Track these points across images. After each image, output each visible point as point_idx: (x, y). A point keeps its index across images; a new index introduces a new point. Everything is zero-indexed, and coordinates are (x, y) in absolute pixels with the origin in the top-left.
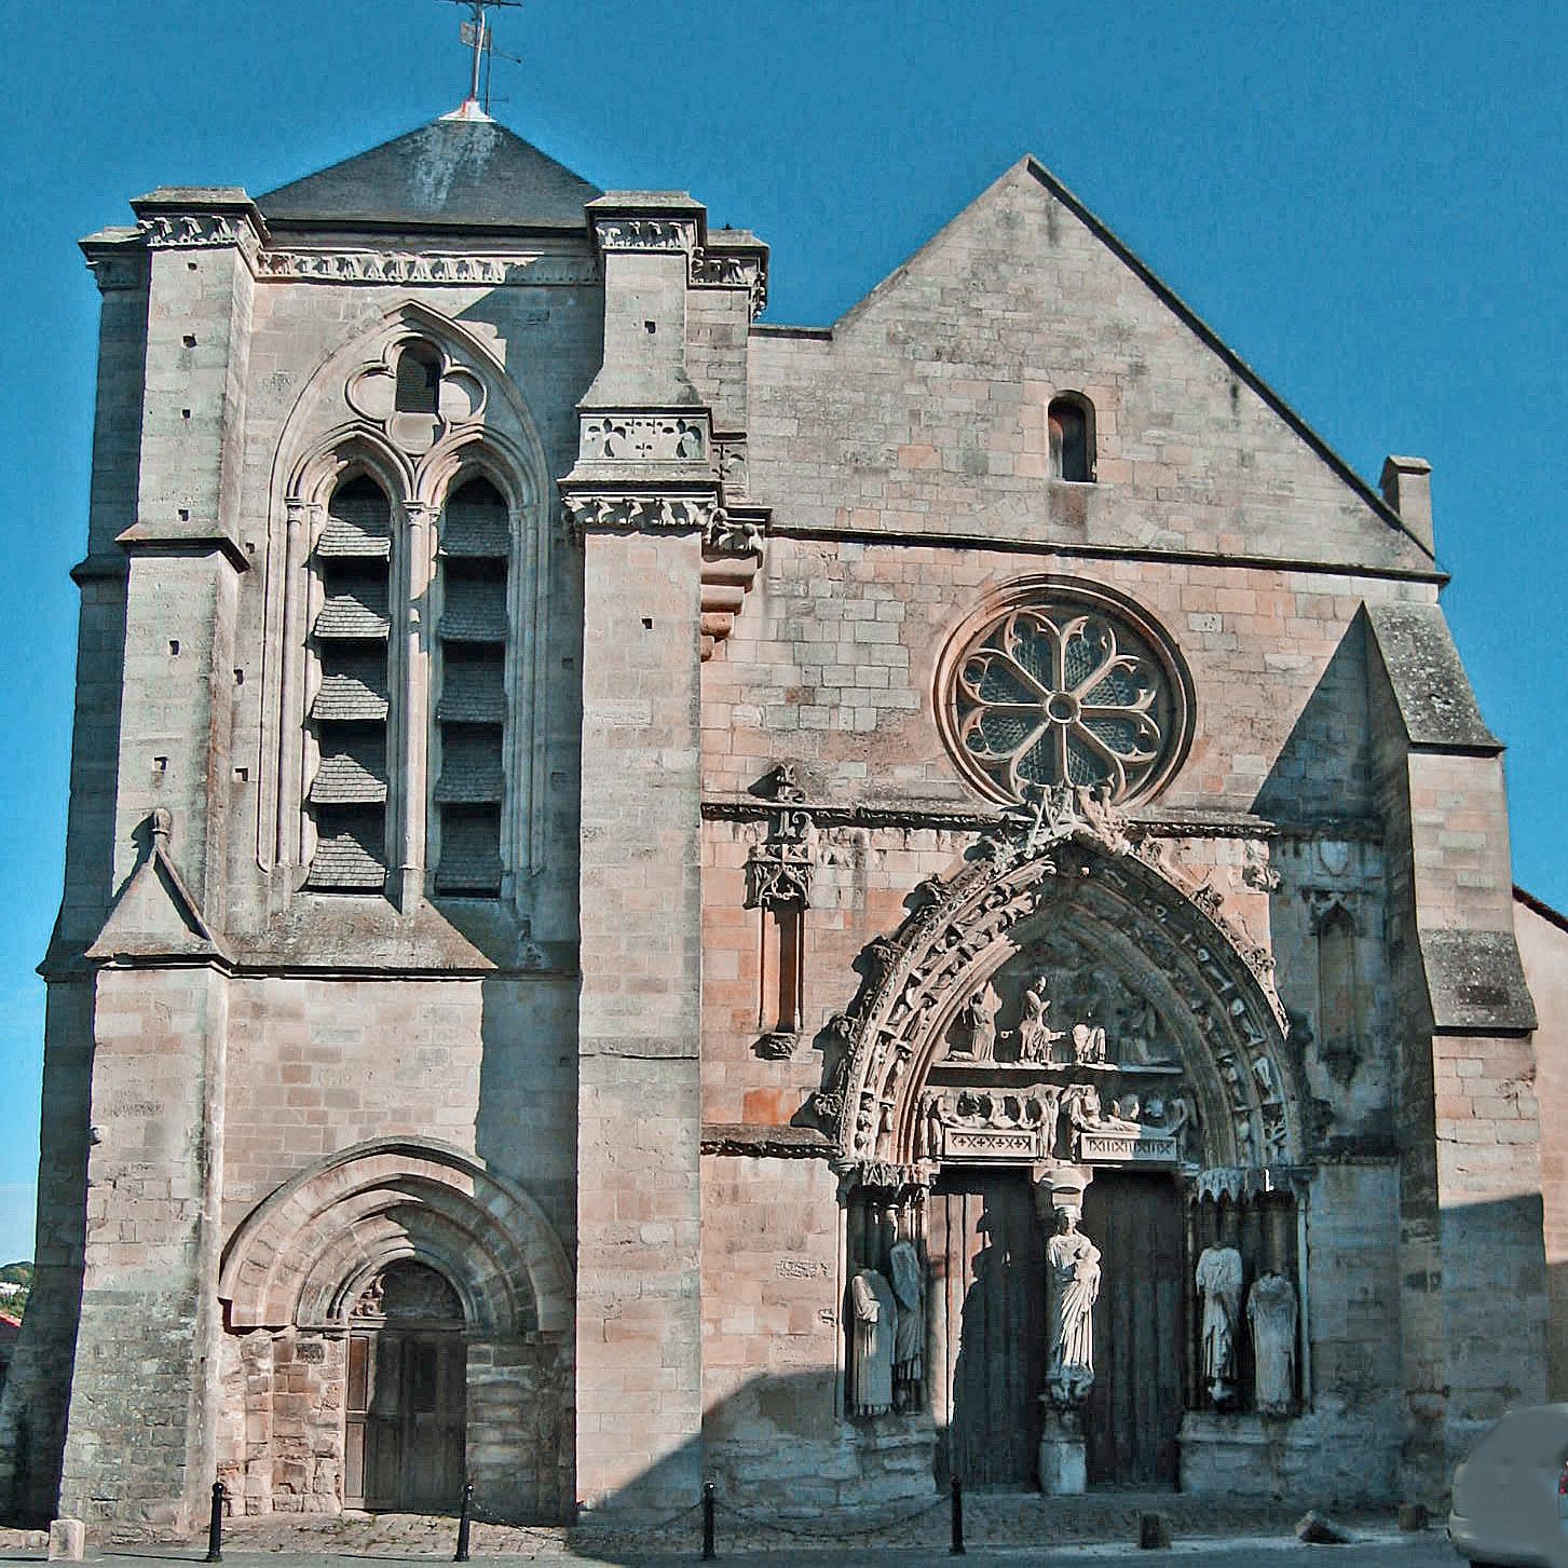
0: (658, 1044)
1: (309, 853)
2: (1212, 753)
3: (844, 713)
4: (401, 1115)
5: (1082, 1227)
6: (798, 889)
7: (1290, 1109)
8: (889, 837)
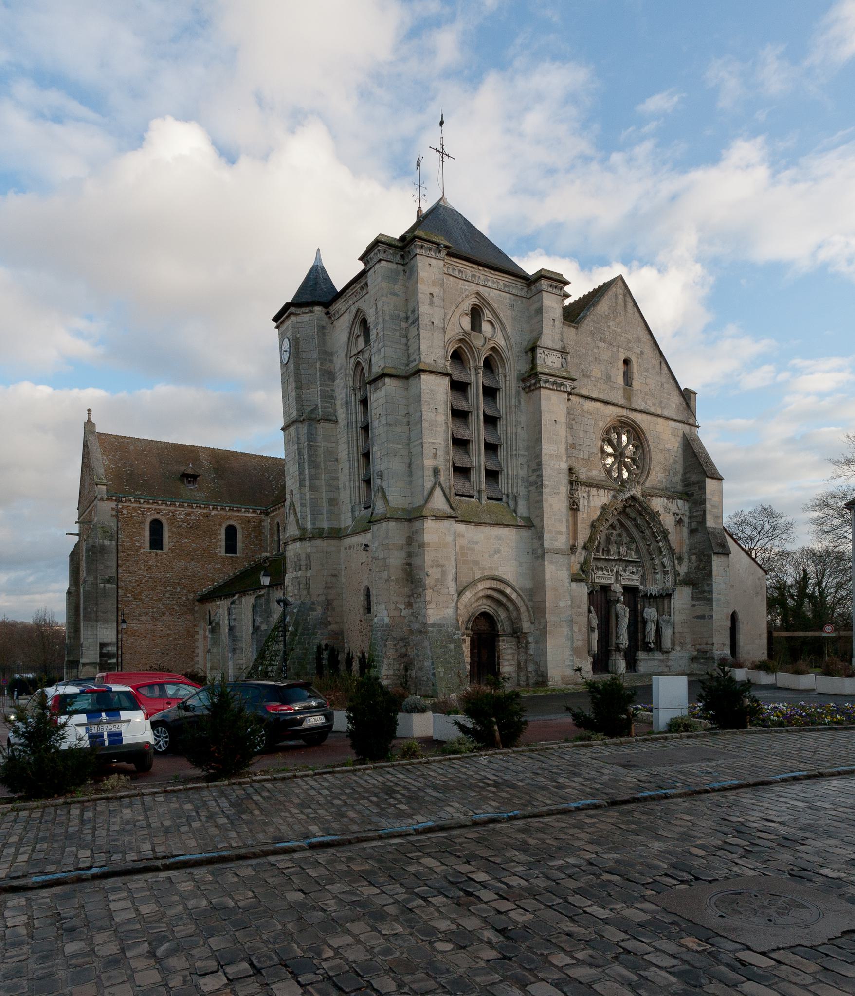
0: (562, 549)
1: (452, 483)
2: (654, 473)
3: (582, 453)
4: (491, 568)
5: (624, 603)
6: (577, 505)
7: (671, 572)
8: (594, 491)
